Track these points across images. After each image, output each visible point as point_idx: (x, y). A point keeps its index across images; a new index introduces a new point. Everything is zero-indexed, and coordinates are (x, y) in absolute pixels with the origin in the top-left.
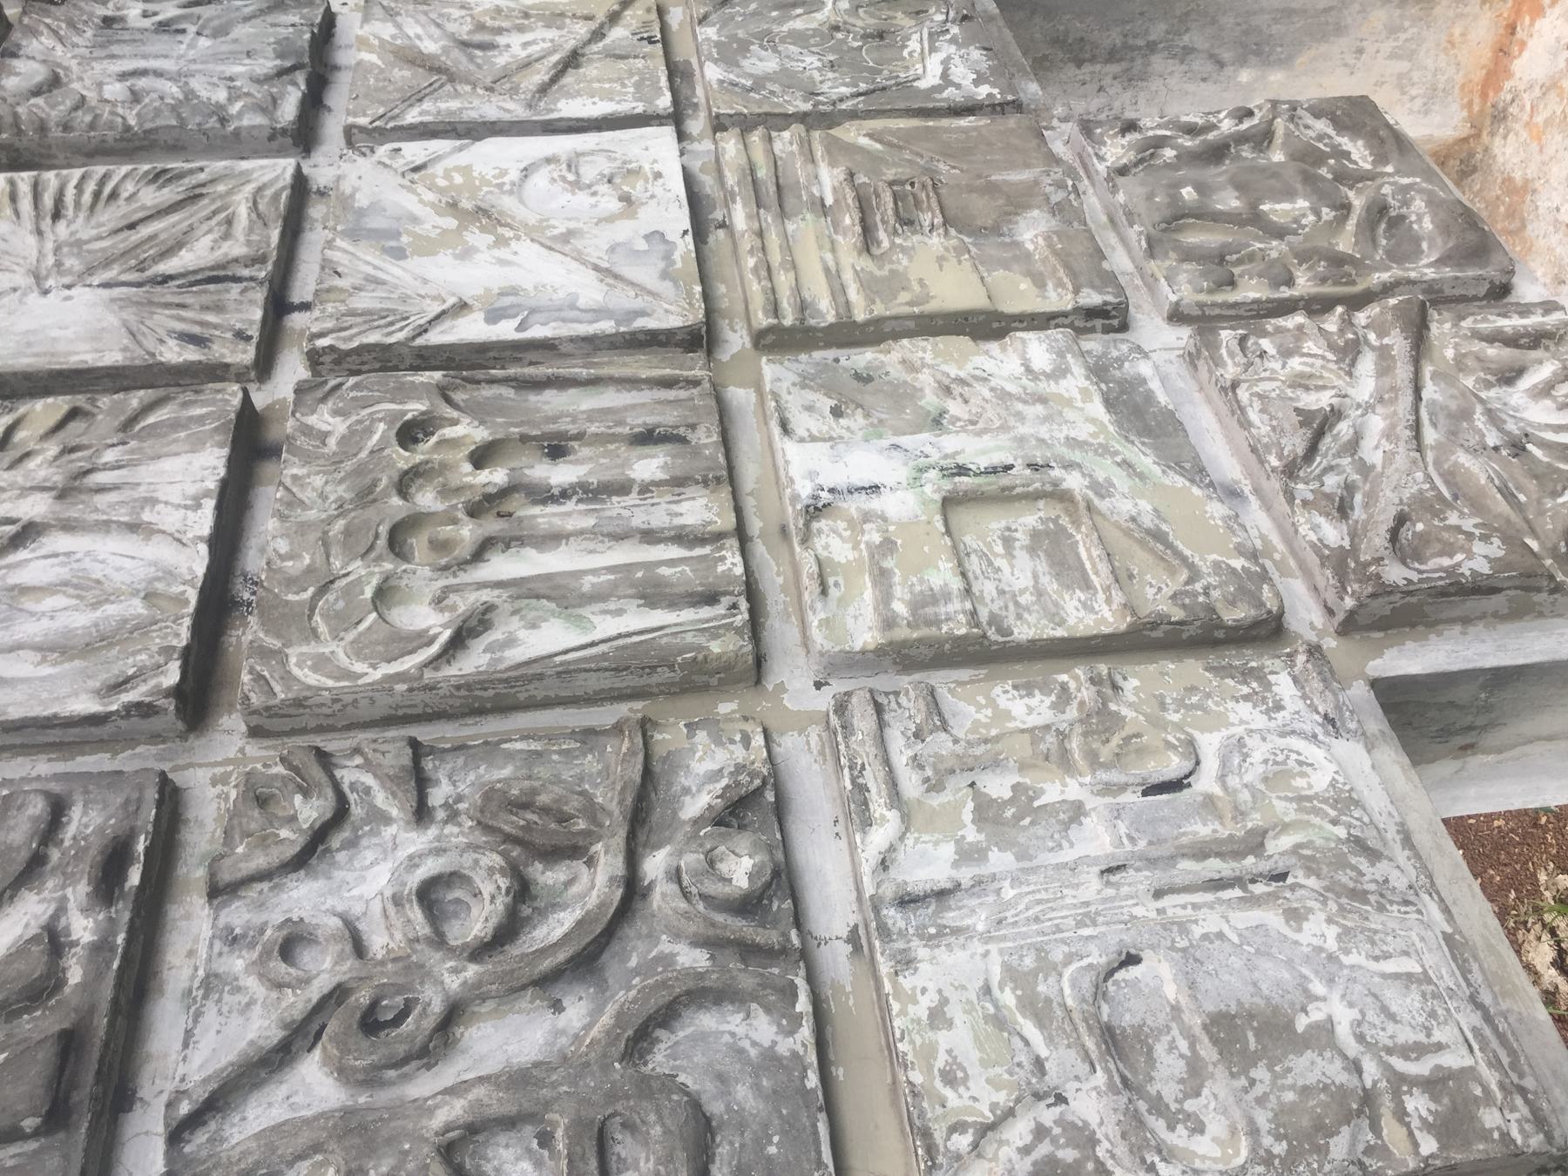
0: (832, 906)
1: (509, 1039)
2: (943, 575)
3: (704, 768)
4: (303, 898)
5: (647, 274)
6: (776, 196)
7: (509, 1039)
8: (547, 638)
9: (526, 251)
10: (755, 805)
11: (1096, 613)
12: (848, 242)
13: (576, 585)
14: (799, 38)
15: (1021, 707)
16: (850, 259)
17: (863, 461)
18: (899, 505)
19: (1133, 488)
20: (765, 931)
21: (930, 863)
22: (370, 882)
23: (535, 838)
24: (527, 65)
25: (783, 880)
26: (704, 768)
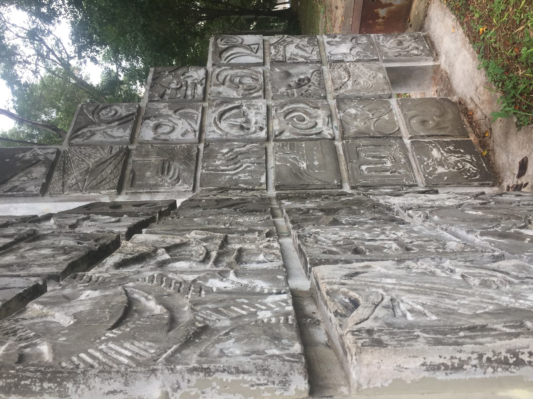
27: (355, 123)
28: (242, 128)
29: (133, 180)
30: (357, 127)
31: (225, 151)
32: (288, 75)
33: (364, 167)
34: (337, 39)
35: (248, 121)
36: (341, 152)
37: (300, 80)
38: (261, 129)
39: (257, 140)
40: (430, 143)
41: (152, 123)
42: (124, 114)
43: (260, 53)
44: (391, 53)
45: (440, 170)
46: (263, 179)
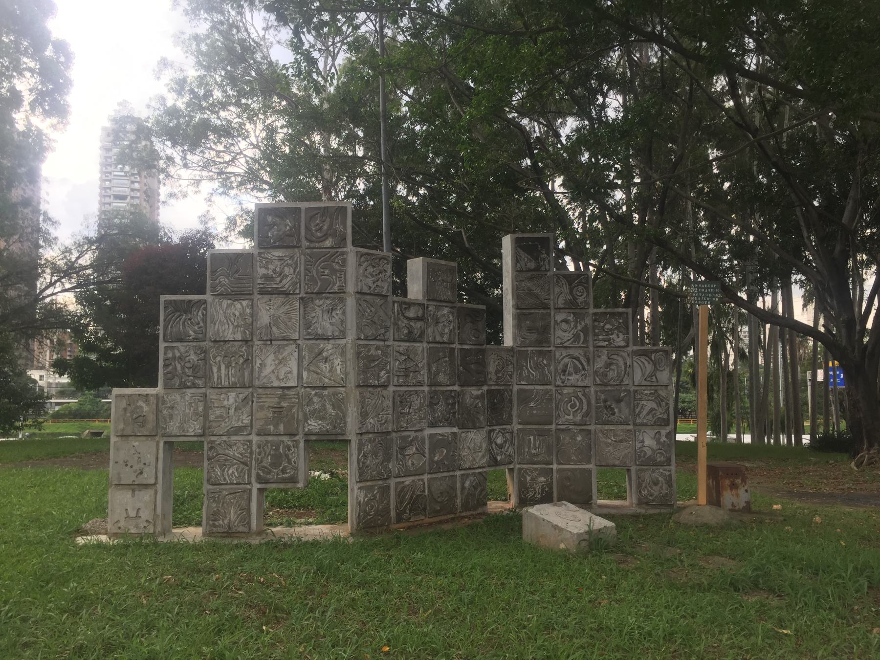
0: (189, 392)
1: (179, 367)
2: (216, 405)
3: (200, 382)
4: (192, 352)
5: (265, 381)
6: (283, 397)
7: (179, 367)
8: (215, 370)
9: (272, 368)
10: (194, 386)
11: (212, 418)
12: (271, 405)
13: (221, 372)
14: (324, 406)
15: (201, 409)
16: (267, 405)
17: (231, 400)
18: (226, 403)
19: (225, 426)
20: (183, 386)
21: (187, 398)
22: (193, 357)
23: (194, 368)
24: (318, 367)
25: (189, 387)
26: (200, 382)
27: (567, 438)
28: (564, 371)
29: (524, 314)
30: (564, 439)
31: (545, 362)
32: (619, 401)
33: (532, 438)
34: (663, 439)
35: (570, 374)
36: (546, 427)
37: (612, 409)
38: (563, 382)
39: (555, 380)
40: (552, 479)
41: (571, 318)
42: (578, 301)
43: (644, 383)
44: (647, 476)
45: (529, 478)
46: (523, 383)
